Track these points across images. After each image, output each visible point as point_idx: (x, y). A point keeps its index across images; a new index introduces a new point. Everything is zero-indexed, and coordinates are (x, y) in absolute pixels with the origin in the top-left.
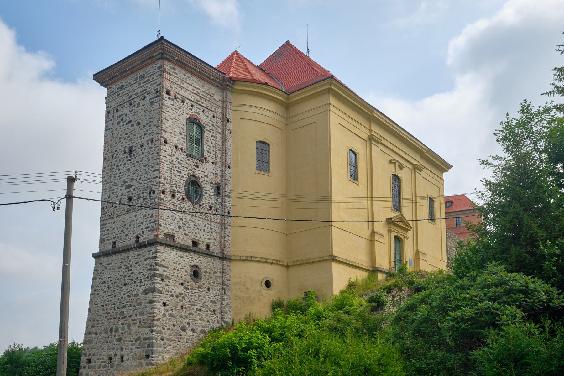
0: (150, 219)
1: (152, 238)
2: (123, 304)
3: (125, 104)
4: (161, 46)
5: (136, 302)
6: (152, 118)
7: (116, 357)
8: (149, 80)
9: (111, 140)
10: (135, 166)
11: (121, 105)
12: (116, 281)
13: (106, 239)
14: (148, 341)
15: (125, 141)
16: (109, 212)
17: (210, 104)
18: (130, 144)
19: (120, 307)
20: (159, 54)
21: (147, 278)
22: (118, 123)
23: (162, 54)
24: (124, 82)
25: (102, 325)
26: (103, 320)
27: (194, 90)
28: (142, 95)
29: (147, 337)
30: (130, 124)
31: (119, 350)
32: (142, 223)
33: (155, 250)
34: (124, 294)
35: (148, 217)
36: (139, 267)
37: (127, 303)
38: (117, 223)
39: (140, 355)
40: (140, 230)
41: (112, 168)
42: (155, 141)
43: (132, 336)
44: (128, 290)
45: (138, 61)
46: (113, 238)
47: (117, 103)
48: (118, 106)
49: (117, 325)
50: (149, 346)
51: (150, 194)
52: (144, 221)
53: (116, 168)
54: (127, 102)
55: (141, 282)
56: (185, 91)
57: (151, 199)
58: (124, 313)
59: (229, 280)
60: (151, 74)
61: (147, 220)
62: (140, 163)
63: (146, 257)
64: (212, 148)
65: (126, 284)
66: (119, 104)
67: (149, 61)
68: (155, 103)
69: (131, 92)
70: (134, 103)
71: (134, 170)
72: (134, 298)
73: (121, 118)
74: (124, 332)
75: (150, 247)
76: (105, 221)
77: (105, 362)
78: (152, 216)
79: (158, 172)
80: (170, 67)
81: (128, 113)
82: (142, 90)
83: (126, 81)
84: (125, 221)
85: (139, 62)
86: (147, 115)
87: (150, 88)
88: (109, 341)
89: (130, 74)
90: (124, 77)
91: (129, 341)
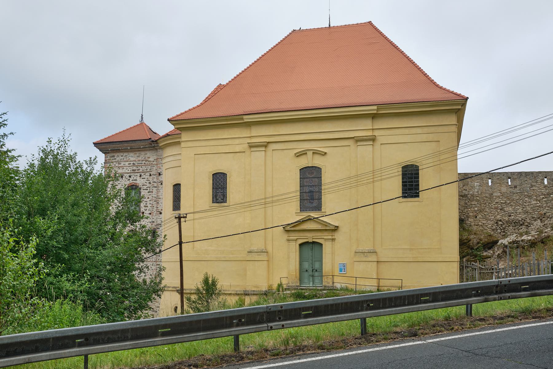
17: (146, 167)
27: (130, 164)
56: (123, 168)
59: (159, 307)
64: (148, 203)
80: (110, 157)
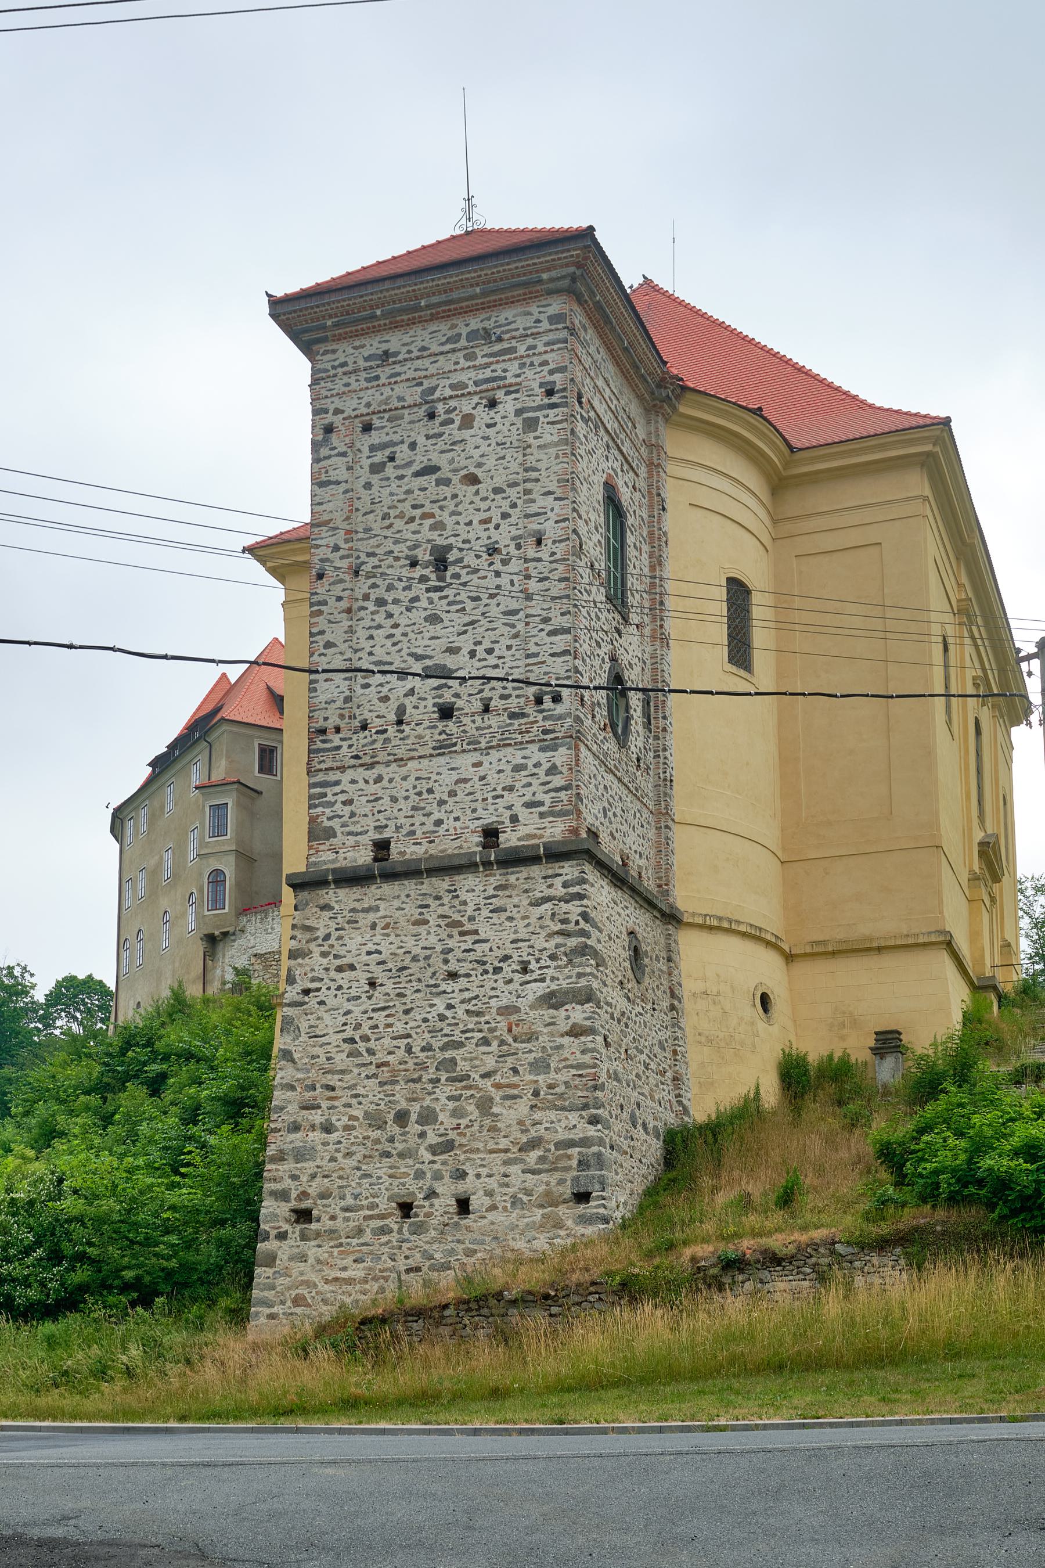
0: (544, 778)
1: (559, 838)
2: (446, 1035)
3: (406, 412)
4: (578, 256)
5: (510, 1030)
6: (537, 470)
7: (436, 1201)
8: (513, 350)
9: (348, 518)
10: (464, 609)
11: (385, 411)
12: (406, 963)
13: (339, 830)
14: (577, 1150)
15: (413, 526)
16: (350, 746)
18: (435, 537)
19: (436, 1044)
20: (563, 277)
21: (553, 957)
22: (376, 468)
23: (574, 280)
24: (395, 341)
25: (354, 1101)
26: (355, 1085)
28: (481, 392)
29: (571, 1136)
30: (434, 477)
31: (447, 1179)
32: (510, 789)
33: (576, 874)
34: (450, 1007)
35: (535, 771)
36: (507, 924)
37: (468, 1035)
38: (391, 781)
39: (548, 1193)
40: (501, 810)
41: (355, 606)
42: (554, 542)
43: (505, 1137)
44: (467, 995)
45: (472, 286)
46: (376, 828)
47: (368, 405)
48: (374, 413)
49: (427, 1102)
50: (583, 1164)
52: (518, 785)
54: (415, 405)
55: (525, 970)
57: (545, 718)
58: (456, 1064)
60: (521, 331)
61: (529, 779)
62: (485, 601)
63: (540, 895)
65: (453, 976)
66: (374, 407)
67: (515, 293)
68: (545, 425)
69: (432, 375)
70: (448, 412)
71: (459, 621)
72: (499, 1018)
73: (387, 452)
74: (464, 1122)
75: (549, 865)
76: (331, 773)
77: (381, 1217)
78: (553, 770)
79: (569, 637)
81: (421, 440)
82: (481, 377)
83: (407, 339)
84: (429, 778)
85: (478, 290)
86: (508, 458)
87: (518, 376)
88: (394, 1152)
89: (426, 321)
91: (491, 1152)
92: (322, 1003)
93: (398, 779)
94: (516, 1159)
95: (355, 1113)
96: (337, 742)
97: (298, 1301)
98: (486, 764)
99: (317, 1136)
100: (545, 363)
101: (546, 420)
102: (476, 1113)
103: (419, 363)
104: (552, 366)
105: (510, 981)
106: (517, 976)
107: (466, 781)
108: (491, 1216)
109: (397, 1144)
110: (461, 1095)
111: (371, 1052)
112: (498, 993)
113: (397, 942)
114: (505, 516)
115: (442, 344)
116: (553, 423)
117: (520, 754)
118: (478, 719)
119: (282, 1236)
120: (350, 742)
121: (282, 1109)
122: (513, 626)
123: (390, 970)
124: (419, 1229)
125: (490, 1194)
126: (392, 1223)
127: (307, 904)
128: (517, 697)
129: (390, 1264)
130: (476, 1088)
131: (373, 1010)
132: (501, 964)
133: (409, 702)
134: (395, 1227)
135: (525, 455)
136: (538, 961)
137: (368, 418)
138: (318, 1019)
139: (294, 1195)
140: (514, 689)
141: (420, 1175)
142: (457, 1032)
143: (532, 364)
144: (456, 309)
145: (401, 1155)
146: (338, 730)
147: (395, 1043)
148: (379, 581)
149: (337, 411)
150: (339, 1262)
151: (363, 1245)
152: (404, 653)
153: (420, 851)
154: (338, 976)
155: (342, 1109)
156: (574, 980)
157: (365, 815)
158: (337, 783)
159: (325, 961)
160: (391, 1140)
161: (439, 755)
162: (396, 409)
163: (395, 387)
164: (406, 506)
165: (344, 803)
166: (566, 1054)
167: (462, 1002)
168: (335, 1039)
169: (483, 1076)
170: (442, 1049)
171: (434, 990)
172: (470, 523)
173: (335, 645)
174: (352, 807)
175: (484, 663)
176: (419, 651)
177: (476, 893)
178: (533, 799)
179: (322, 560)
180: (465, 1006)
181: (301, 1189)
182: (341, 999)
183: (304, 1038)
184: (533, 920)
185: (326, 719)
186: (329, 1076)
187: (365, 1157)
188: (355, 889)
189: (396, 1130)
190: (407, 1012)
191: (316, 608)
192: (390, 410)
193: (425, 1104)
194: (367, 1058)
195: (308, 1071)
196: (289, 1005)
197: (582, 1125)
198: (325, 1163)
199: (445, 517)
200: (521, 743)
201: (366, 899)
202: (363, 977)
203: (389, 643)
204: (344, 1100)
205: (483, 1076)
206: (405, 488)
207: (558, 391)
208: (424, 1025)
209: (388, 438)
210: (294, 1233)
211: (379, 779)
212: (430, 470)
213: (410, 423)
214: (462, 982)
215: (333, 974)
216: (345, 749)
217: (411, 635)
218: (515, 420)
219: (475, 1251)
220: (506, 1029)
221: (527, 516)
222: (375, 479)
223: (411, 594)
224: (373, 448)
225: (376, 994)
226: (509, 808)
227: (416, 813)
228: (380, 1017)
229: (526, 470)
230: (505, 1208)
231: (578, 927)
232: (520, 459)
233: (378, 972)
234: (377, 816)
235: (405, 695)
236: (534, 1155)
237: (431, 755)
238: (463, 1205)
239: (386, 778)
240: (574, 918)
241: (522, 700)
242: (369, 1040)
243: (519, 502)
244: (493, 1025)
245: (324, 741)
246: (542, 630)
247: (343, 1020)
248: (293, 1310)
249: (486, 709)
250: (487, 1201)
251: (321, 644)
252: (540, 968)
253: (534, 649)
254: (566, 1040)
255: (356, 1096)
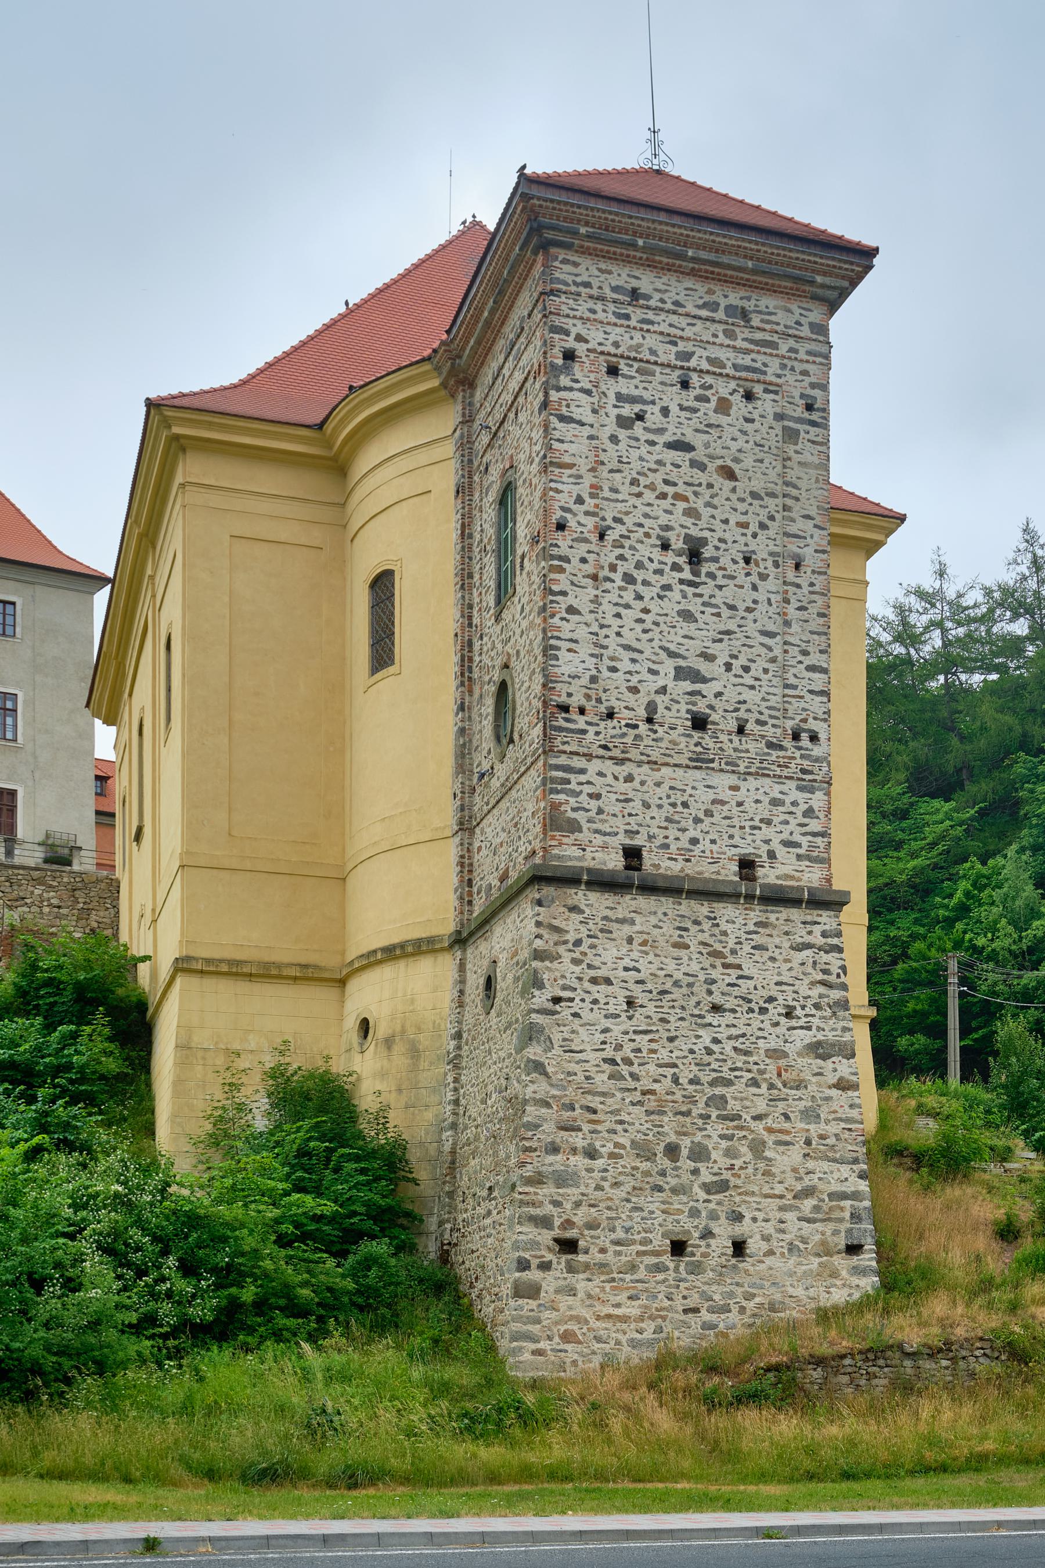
2: (714, 1070)
3: (658, 369)
5: (779, 1075)
6: (795, 487)
7: (712, 1242)
8: (773, 345)
9: (593, 470)
11: (635, 359)
12: (668, 986)
13: (585, 826)
15: (665, 504)
16: (597, 733)
18: (689, 525)
19: (706, 1077)
21: (817, 1006)
25: (619, 1128)
28: (739, 378)
31: (723, 1220)
32: (769, 822)
33: (834, 926)
35: (793, 809)
36: (769, 963)
39: (823, 1243)
40: (758, 842)
42: (813, 572)
44: (734, 1032)
46: (626, 831)
48: (622, 357)
49: (698, 1137)
51: (796, 737)
52: (776, 820)
53: (619, 583)
54: (669, 366)
55: (788, 1015)
57: (802, 757)
61: (787, 817)
63: (800, 940)
65: (716, 1008)
69: (689, 339)
71: (714, 626)
72: (768, 1061)
73: (637, 408)
74: (738, 1163)
76: (576, 758)
77: (656, 1254)
78: (809, 813)
81: (674, 409)
82: (740, 361)
87: (779, 376)
88: (667, 1187)
89: (682, 273)
90: (651, 265)
91: (767, 1196)
92: (576, 1015)
93: (650, 783)
94: (791, 1206)
95: (621, 1140)
96: (581, 725)
97: (567, 1337)
98: (743, 790)
99: (579, 1162)
100: (805, 373)
101: (807, 436)
102: (748, 1157)
103: (674, 319)
104: (813, 379)
105: (777, 1024)
106: (783, 1020)
107: (723, 803)
108: (769, 1261)
109: (669, 1179)
110: (733, 1135)
111: (634, 1077)
112: (766, 1035)
113: (657, 961)
114: (763, 526)
115: (699, 307)
116: (813, 442)
117: (777, 788)
118: (735, 739)
119: (545, 1266)
120: (596, 729)
121: (537, 1126)
122: (770, 649)
123: (650, 992)
124: (696, 1269)
125: (766, 1238)
126: (667, 1259)
127: (553, 901)
128: (773, 726)
129: (667, 1303)
130: (749, 1129)
131: (635, 1032)
132: (766, 1005)
133: (661, 701)
134: (671, 1265)
135: (784, 467)
136: (803, 1007)
137: (614, 359)
138: (573, 1032)
139: (557, 1222)
140: (771, 717)
141: (694, 1213)
142: (725, 1069)
143: (792, 369)
144: (719, 274)
145: (674, 1191)
146: (582, 711)
147: (661, 1070)
148: (627, 552)
149: (579, 338)
150: (611, 1298)
151: (638, 1281)
152: (656, 643)
153: (675, 868)
154: (594, 988)
155: (606, 1135)
156: (839, 1033)
157: (614, 815)
158: (583, 771)
159: (577, 969)
160: (663, 1173)
161: (696, 768)
162: (648, 362)
163: (647, 335)
164: (658, 478)
165: (591, 796)
166: (835, 1106)
167: (730, 1038)
168: (594, 1058)
169: (755, 1118)
170: (713, 1083)
171: (699, 1021)
172: (726, 522)
173: (578, 613)
174: (600, 803)
175: (740, 680)
176: (672, 647)
177: (737, 926)
178: (791, 838)
179: (563, 509)
180: (732, 1043)
181: (565, 1217)
182: (597, 1015)
183: (557, 1051)
184: (795, 964)
185: (570, 695)
186: (589, 1097)
187: (634, 1188)
188: (606, 895)
189: (667, 1163)
190: (671, 1039)
191: (556, 563)
192: (641, 360)
193: (697, 1139)
194: (631, 1084)
195: (564, 1089)
196: (538, 1012)
197: (853, 1178)
198: (590, 1190)
199: (699, 504)
200: (780, 777)
201: (620, 909)
202: (622, 996)
203: (639, 628)
204: (607, 1125)
205: (755, 1118)
206: (655, 457)
207: (818, 410)
208: (691, 1056)
209: (636, 393)
210: (559, 1263)
211: (629, 779)
212: (680, 446)
213: (662, 383)
214: (729, 1018)
215: (587, 985)
216: (590, 736)
217: (663, 627)
218: (774, 424)
219: (754, 1295)
220: (775, 1073)
221: (786, 534)
222: (622, 434)
223: (664, 580)
224: (619, 397)
225: (637, 1015)
226: (767, 842)
227: (670, 826)
228: (642, 1040)
229: (787, 484)
230: (782, 1254)
231: (839, 981)
232: (779, 469)
233: (637, 991)
234: (628, 819)
235: (657, 692)
236: (808, 1204)
237: (688, 767)
238: (739, 1248)
239: (638, 780)
240: (835, 970)
241: (779, 731)
242: (631, 1064)
243: (777, 516)
244: (762, 1067)
245: (567, 720)
246: (800, 662)
247: (602, 1037)
248: (562, 1347)
249: (741, 730)
250: (764, 1246)
251: (564, 606)
252: (806, 1016)
253: (792, 681)
254: (834, 1092)
255: (621, 1122)
